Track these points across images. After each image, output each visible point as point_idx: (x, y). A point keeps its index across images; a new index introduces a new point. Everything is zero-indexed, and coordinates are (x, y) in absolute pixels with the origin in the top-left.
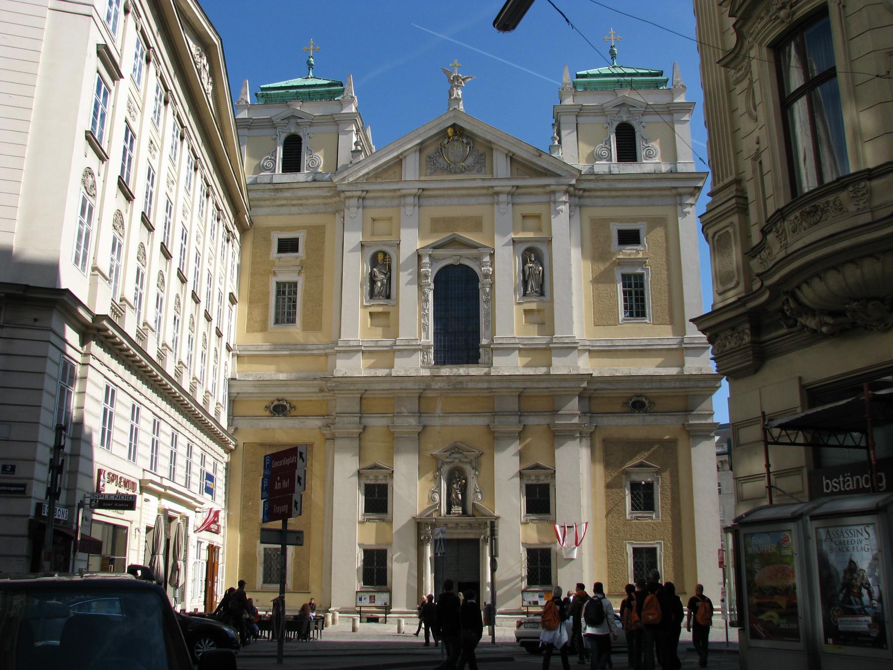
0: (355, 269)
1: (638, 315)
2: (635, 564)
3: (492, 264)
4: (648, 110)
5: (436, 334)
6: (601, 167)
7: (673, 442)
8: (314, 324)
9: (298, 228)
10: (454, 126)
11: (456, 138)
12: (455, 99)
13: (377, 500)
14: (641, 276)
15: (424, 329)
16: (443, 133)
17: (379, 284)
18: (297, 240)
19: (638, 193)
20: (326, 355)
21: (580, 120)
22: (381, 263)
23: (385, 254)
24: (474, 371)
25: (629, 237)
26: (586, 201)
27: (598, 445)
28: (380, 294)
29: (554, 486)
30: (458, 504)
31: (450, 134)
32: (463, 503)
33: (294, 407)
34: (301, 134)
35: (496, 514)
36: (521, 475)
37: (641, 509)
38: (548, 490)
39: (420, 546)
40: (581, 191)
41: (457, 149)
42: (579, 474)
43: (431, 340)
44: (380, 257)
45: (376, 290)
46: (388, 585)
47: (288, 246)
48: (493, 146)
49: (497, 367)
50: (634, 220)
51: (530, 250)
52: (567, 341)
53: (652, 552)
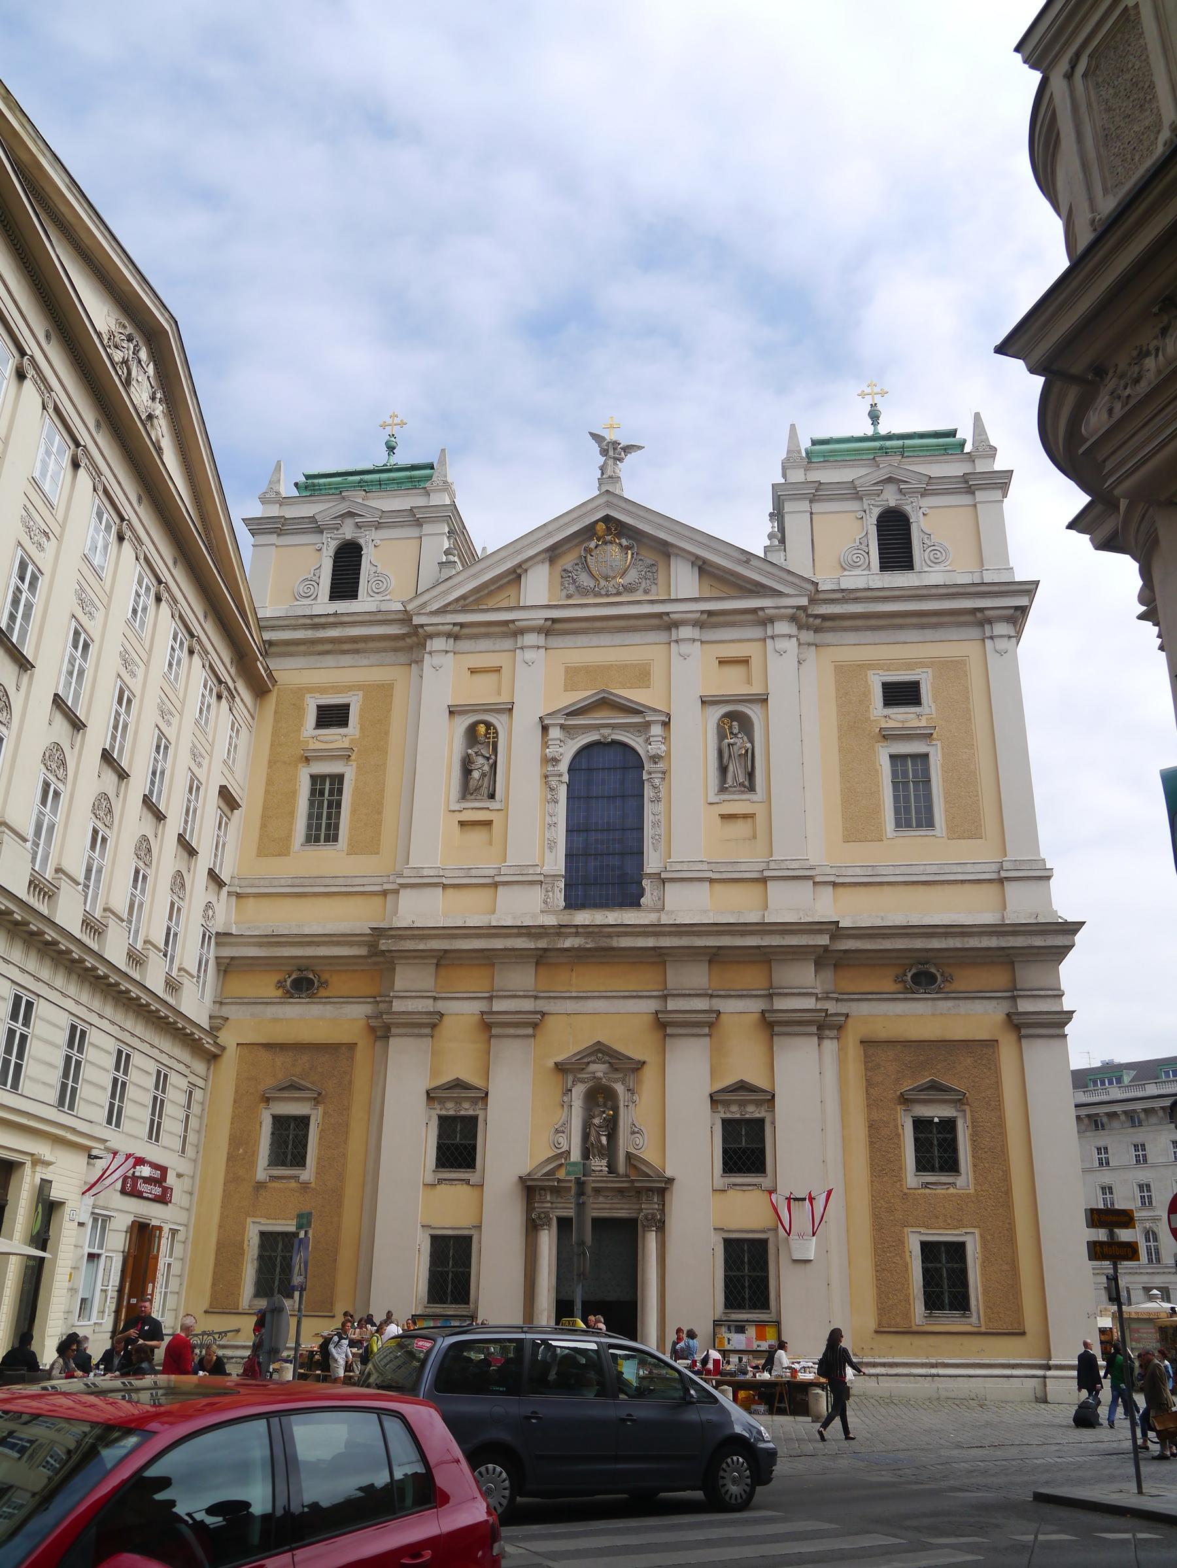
0: (439, 747)
1: (919, 825)
2: (926, 1272)
3: (666, 739)
5: (569, 856)
6: (853, 581)
7: (993, 1043)
9: (350, 688)
10: (607, 519)
11: (609, 538)
12: (610, 477)
13: (458, 1149)
14: (925, 757)
15: (551, 848)
16: (589, 532)
17: (476, 774)
18: (346, 707)
20: (385, 893)
21: (817, 507)
22: (481, 738)
23: (488, 725)
24: (629, 917)
25: (902, 694)
26: (829, 637)
28: (478, 789)
29: (773, 1123)
30: (601, 1155)
31: (600, 533)
32: (610, 1152)
33: (326, 982)
34: (362, 541)
35: (669, 1173)
36: (715, 1100)
37: (933, 1170)
39: (532, 1227)
40: (820, 617)
41: (613, 554)
42: (816, 1103)
43: (560, 867)
44: (482, 729)
45: (473, 784)
46: (472, 1306)
48: (671, 550)
49: (672, 912)
50: (909, 665)
51: (731, 716)
52: (794, 865)
53: (957, 1250)
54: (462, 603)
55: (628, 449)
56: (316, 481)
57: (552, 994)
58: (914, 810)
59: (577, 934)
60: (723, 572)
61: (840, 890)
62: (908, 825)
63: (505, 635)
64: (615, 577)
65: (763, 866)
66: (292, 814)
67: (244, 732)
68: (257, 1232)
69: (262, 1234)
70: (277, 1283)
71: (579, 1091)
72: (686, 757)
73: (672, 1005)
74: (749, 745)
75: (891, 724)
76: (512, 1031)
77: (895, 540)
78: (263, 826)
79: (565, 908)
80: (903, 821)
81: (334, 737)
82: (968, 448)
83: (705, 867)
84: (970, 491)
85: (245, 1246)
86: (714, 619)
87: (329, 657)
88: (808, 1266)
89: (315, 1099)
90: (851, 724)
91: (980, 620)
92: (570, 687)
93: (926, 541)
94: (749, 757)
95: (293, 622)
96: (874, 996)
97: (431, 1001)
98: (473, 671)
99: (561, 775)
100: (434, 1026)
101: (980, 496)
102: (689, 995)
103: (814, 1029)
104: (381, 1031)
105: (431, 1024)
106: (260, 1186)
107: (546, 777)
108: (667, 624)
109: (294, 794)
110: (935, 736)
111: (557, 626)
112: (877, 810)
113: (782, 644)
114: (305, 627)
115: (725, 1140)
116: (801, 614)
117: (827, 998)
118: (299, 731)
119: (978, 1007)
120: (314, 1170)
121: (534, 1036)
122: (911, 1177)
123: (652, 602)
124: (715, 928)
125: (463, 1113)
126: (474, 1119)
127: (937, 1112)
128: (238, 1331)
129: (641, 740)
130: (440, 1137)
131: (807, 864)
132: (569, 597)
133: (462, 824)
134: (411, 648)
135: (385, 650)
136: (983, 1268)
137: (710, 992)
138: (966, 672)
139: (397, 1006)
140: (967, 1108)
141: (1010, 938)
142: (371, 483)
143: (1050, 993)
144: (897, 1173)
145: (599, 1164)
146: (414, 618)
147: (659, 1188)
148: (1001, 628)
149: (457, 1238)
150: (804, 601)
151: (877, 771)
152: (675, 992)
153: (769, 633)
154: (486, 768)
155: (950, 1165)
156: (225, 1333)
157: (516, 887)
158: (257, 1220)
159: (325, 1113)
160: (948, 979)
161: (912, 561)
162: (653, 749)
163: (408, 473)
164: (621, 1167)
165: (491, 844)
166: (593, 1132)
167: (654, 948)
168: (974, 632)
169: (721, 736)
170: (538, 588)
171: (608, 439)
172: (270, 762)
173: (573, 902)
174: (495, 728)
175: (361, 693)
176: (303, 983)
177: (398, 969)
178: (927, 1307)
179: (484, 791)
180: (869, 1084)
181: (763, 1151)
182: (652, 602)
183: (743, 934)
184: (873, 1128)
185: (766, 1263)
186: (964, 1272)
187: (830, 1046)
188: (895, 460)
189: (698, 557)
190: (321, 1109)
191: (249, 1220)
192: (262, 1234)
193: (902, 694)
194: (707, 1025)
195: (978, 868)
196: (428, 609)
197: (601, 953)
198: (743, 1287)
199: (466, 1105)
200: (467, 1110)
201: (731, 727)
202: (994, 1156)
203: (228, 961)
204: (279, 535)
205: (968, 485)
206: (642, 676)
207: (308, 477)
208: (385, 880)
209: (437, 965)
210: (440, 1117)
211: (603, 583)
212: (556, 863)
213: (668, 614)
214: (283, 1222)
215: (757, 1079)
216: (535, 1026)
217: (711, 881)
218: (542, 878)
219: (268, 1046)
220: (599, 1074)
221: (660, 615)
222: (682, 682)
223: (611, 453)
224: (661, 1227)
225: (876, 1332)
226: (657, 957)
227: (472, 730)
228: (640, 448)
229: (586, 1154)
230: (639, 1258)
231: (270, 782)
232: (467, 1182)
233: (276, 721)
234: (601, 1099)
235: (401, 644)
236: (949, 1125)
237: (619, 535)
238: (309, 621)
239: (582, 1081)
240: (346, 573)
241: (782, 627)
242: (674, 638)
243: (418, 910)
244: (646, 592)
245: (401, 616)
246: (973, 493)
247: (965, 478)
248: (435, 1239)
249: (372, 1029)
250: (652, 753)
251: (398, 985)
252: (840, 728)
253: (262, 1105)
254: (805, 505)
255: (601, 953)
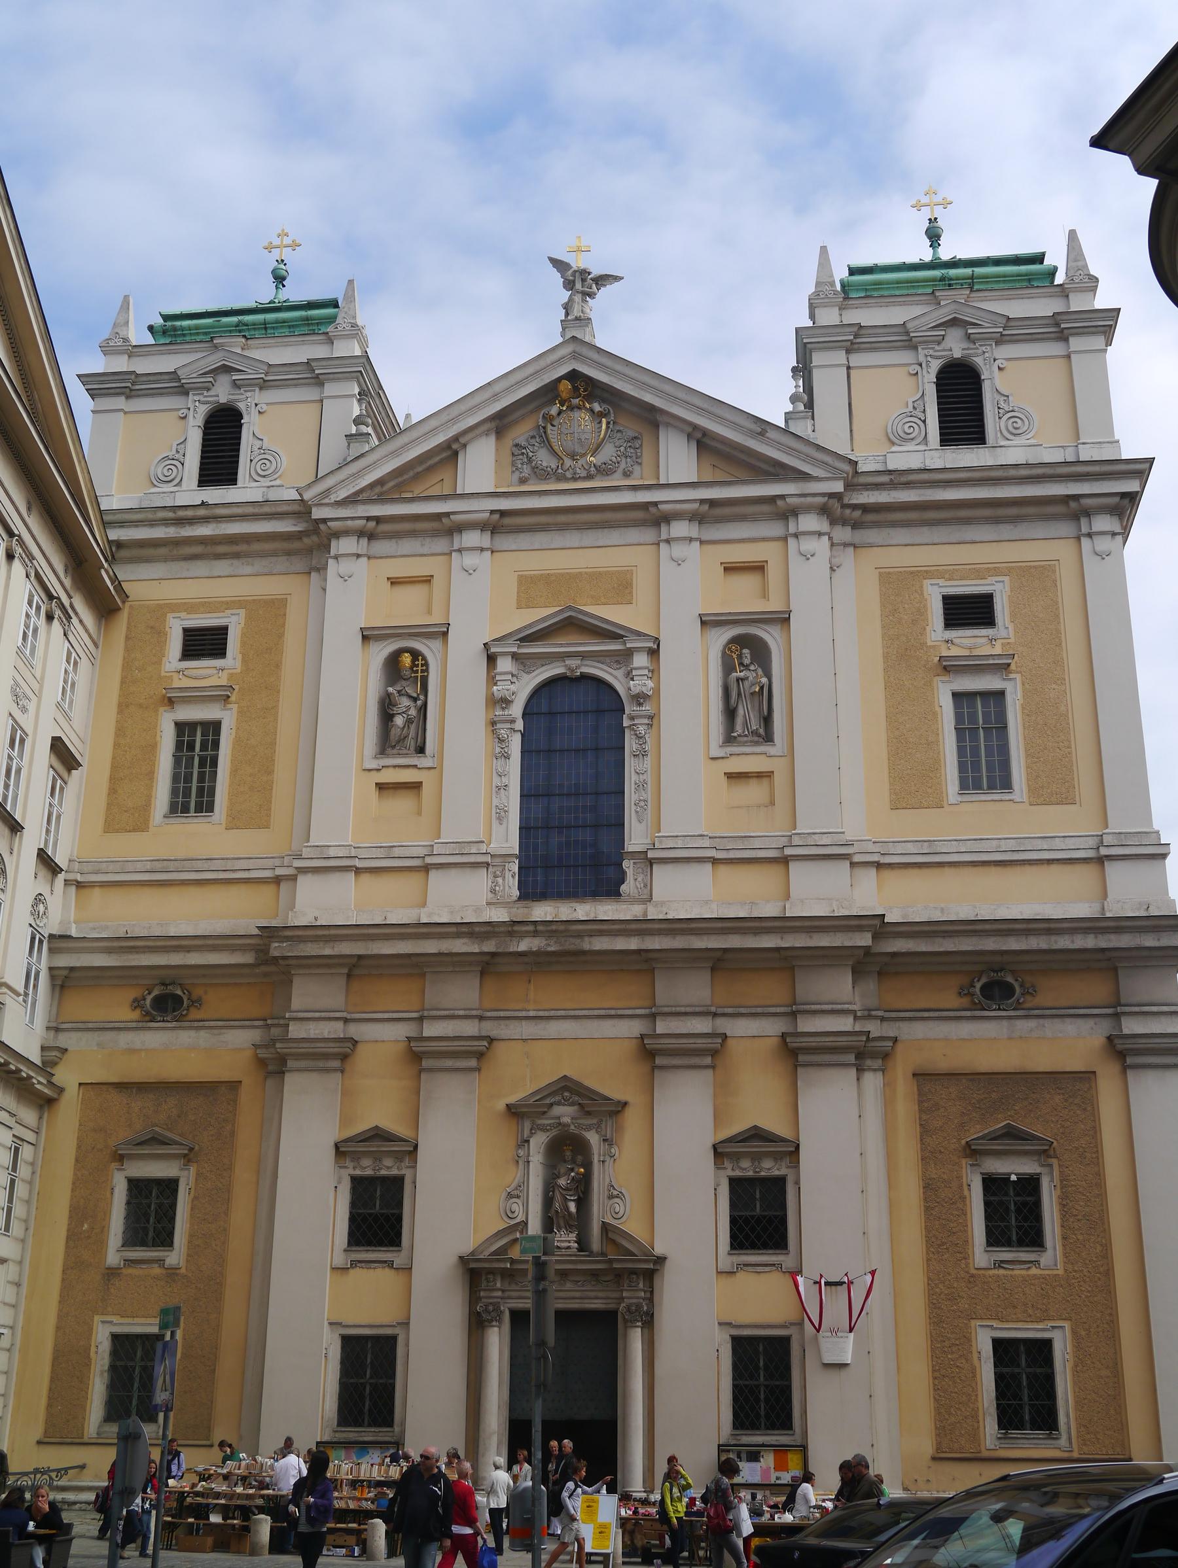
0: (349, 686)
1: (992, 787)
2: (999, 1378)
3: (654, 673)
4: (1010, 332)
5: (525, 829)
6: (905, 459)
7: (1088, 1076)
8: (255, 815)
10: (573, 376)
11: (576, 401)
12: (577, 319)
13: (377, 1220)
15: (500, 819)
16: (549, 393)
17: (399, 721)
18: (224, 630)
19: (987, 512)
20: (277, 880)
21: (857, 359)
22: (405, 673)
23: (415, 654)
24: (606, 910)
25: (969, 611)
26: (871, 535)
27: (904, 1087)
28: (402, 740)
29: (797, 1182)
30: (569, 1227)
31: (564, 395)
32: (580, 1223)
34: (242, 406)
35: (659, 1250)
36: (720, 1153)
37: (1008, 1243)
38: (783, 1192)
39: (477, 1323)
40: (860, 508)
41: (582, 424)
42: (854, 1157)
43: (513, 844)
44: (407, 659)
45: (395, 733)
46: (397, 1429)
47: (205, 643)
48: (659, 418)
49: (663, 903)
50: (980, 573)
51: (740, 641)
52: (825, 840)
53: (1042, 1350)
54: (378, 490)
55: (602, 280)
56: (178, 323)
57: (502, 1014)
58: (985, 768)
59: (536, 934)
60: (732, 450)
61: (887, 874)
62: (977, 786)
63: (435, 534)
64: (584, 455)
65: (783, 842)
66: (151, 775)
67: (84, 664)
68: (107, 1334)
69: (115, 1337)
70: (134, 1402)
71: (538, 1142)
72: (682, 694)
73: (662, 1027)
74: (764, 680)
75: (955, 651)
76: (449, 1063)
77: (961, 404)
78: (112, 791)
79: (520, 898)
80: (970, 782)
81: (207, 672)
82: (1060, 279)
83: (706, 843)
84: (1062, 336)
85: (92, 1354)
86: (718, 511)
87: (199, 563)
88: (844, 1373)
89: (185, 1156)
90: (901, 653)
91: (1074, 511)
92: (524, 602)
93: (1002, 405)
94: (764, 695)
95: (150, 516)
96: (932, 1014)
97: (340, 1025)
98: (394, 582)
99: (513, 721)
100: (344, 1057)
101: (1075, 343)
102: (686, 1014)
103: (851, 1058)
104: (274, 1065)
105: (339, 1055)
106: (112, 1273)
107: (493, 723)
108: (654, 518)
109: (152, 748)
110: (1013, 667)
111: (507, 521)
112: (936, 765)
113: (808, 545)
114: (165, 522)
115: (733, 1205)
116: (835, 504)
117: (869, 1017)
118: (159, 663)
119: (1070, 1028)
120: (184, 1250)
121: (479, 1070)
122: (980, 1255)
123: (635, 488)
124: (719, 925)
125: (383, 1172)
126: (399, 1181)
127: (1014, 1167)
128: (83, 1467)
129: (620, 673)
130: (353, 1204)
131: (841, 839)
132: (523, 481)
133: (381, 787)
134: (309, 551)
135: (274, 554)
136: (1076, 1371)
137: (713, 1009)
138: (1055, 581)
139: (296, 1031)
140: (1054, 1162)
141: (1112, 937)
142: (254, 326)
143: (1165, 1009)
144: (963, 1250)
145: (565, 1239)
146: (314, 510)
147: (646, 1270)
148: (1103, 523)
149: (377, 1339)
150: (839, 487)
151: (935, 714)
152: (666, 1010)
153: (792, 529)
154: (413, 712)
155: (1033, 1238)
156: (66, 1469)
157: (453, 872)
158: (108, 1318)
159: (199, 1175)
160: (1030, 991)
161: (983, 432)
162: (637, 685)
163: (302, 313)
164: (596, 1244)
165: (419, 813)
166: (558, 1196)
167: (639, 952)
168: (1065, 528)
169: (728, 668)
170: (481, 469)
171: (574, 266)
172: (120, 705)
173: (530, 892)
174: (424, 658)
175: (242, 612)
176: (168, 1001)
177: (297, 982)
178: (1002, 1424)
179: (410, 742)
180: (925, 1131)
181: (783, 1220)
182: (635, 488)
183: (757, 932)
184: (929, 1187)
185: (788, 1368)
186: (1050, 1378)
187: (872, 1081)
188: (962, 295)
189: (695, 427)
190: (193, 1169)
191: (97, 1318)
192: (115, 1337)
193: (969, 611)
194: (710, 1053)
195: (1071, 844)
196: (333, 498)
197: (569, 959)
198: (758, 1400)
199: (388, 1162)
200: (388, 1168)
201: (740, 657)
202: (1090, 1224)
203: (65, 973)
204: (128, 397)
205: (1060, 329)
206: (621, 587)
207: (166, 318)
208: (277, 862)
209: (349, 976)
210: (354, 1179)
211: (568, 462)
212: (507, 838)
213: (655, 504)
214: (142, 1320)
215: (775, 1124)
216: (480, 1056)
217: (715, 861)
218: (488, 859)
219: (121, 1086)
220: (566, 1120)
221: (645, 506)
222: (676, 595)
223: (578, 286)
224: (648, 1322)
225: (934, 1459)
226: (642, 961)
227: (393, 661)
228: (617, 279)
229: (549, 1225)
230: (620, 1362)
231: (120, 731)
232: (390, 1264)
233: (127, 650)
234: (568, 1151)
235: (296, 545)
236: (1030, 1184)
237: (590, 398)
238: (171, 515)
239: (543, 1129)
240: (221, 451)
241: (810, 522)
242: (664, 536)
243: (321, 903)
244: (627, 474)
245: (296, 508)
246: (1066, 340)
247: (1055, 319)
248: (346, 1340)
249: (262, 1063)
250: (635, 691)
251: (296, 1003)
252: (886, 657)
253: (114, 1165)
254: (840, 357)
255: (569, 959)
